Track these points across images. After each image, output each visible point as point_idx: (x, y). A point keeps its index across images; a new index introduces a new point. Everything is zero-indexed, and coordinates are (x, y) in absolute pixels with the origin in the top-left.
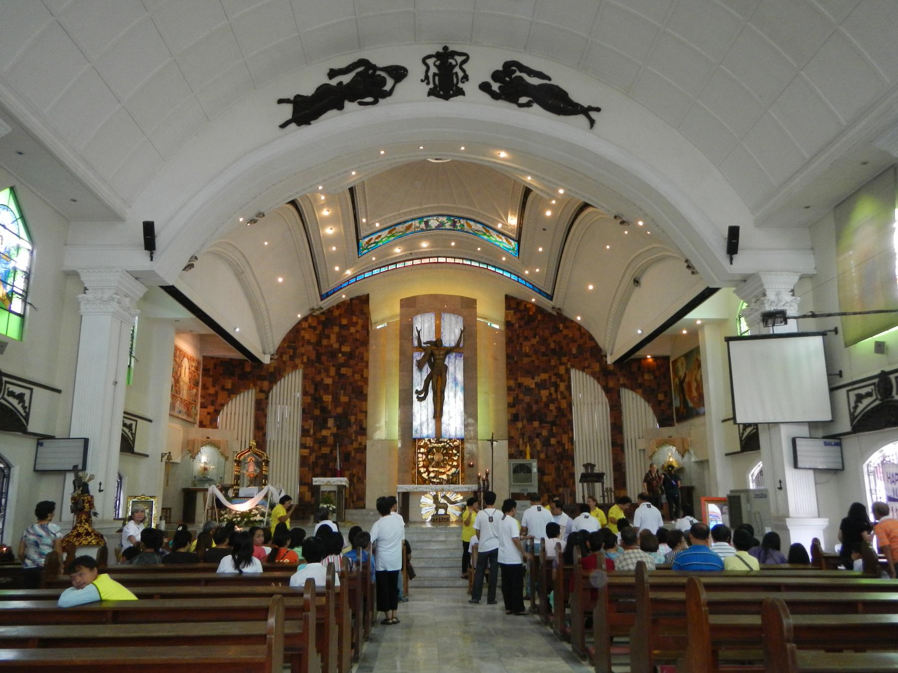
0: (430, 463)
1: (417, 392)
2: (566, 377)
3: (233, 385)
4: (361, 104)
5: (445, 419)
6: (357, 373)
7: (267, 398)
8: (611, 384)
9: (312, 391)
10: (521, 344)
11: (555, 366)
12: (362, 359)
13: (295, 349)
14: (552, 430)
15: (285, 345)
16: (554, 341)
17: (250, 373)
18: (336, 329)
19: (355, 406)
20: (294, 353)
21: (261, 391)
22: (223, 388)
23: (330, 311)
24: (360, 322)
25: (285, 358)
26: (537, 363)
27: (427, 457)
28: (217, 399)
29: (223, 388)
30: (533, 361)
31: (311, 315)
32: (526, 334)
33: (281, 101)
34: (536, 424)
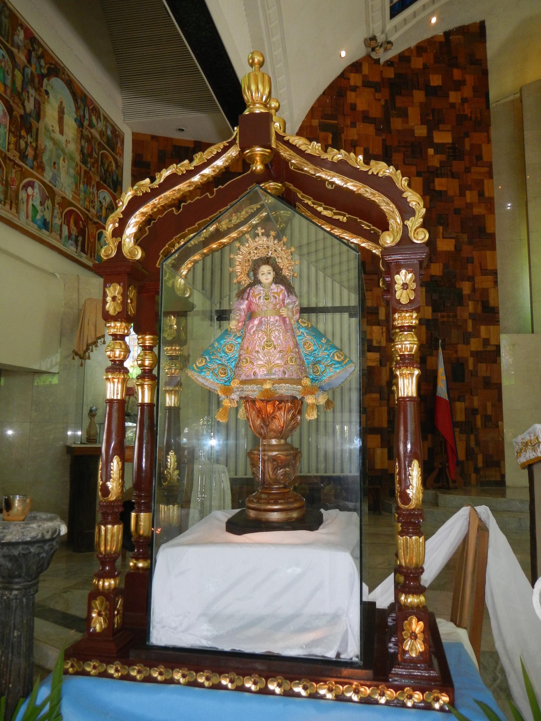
6: (470, 188)
12: (479, 157)
15: (315, 122)
18: (419, 96)
19: (470, 260)
24: (470, 80)
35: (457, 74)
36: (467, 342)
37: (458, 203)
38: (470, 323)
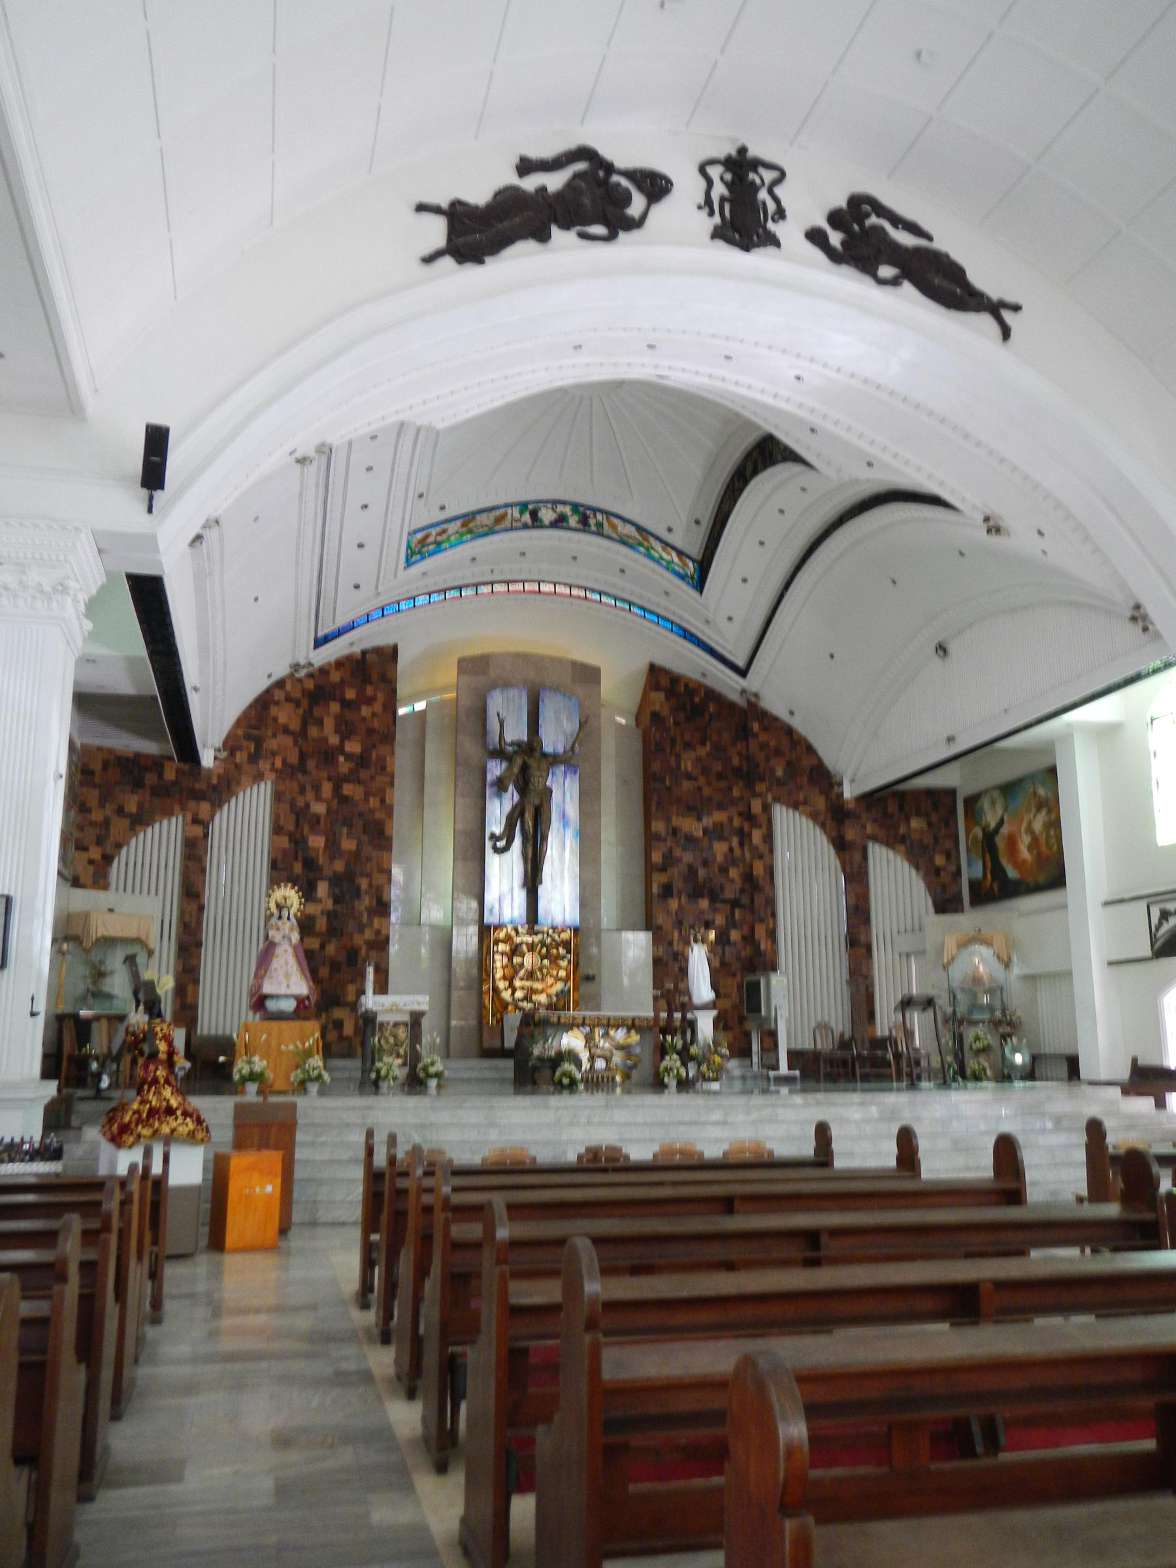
0: (516, 972)
1: (493, 836)
2: (763, 819)
3: (140, 806)
4: (583, 236)
5: (541, 890)
6: (374, 795)
7: (206, 836)
8: (850, 834)
9: (290, 827)
10: (678, 756)
11: (742, 798)
12: (383, 768)
13: (259, 742)
14: (733, 914)
15: (240, 732)
16: (739, 754)
17: (174, 783)
18: (335, 707)
20: (258, 747)
21: (196, 821)
22: (120, 811)
23: (323, 671)
24: (380, 697)
25: (240, 757)
26: (707, 791)
27: (510, 959)
28: (108, 834)
29: (120, 811)
30: (700, 789)
31: (291, 675)
32: (687, 737)
33: (421, 208)
34: (704, 903)
35: (369, 690)
36: (361, 931)
37: (362, 807)
38: (365, 915)
